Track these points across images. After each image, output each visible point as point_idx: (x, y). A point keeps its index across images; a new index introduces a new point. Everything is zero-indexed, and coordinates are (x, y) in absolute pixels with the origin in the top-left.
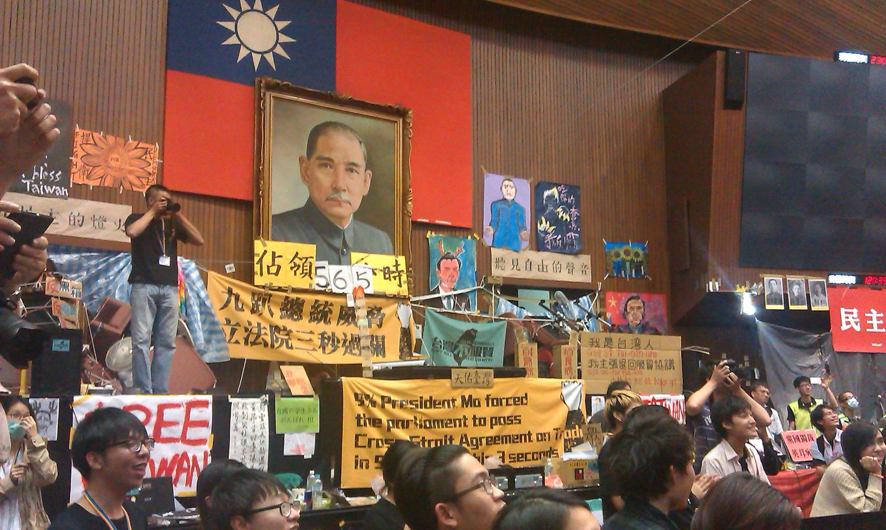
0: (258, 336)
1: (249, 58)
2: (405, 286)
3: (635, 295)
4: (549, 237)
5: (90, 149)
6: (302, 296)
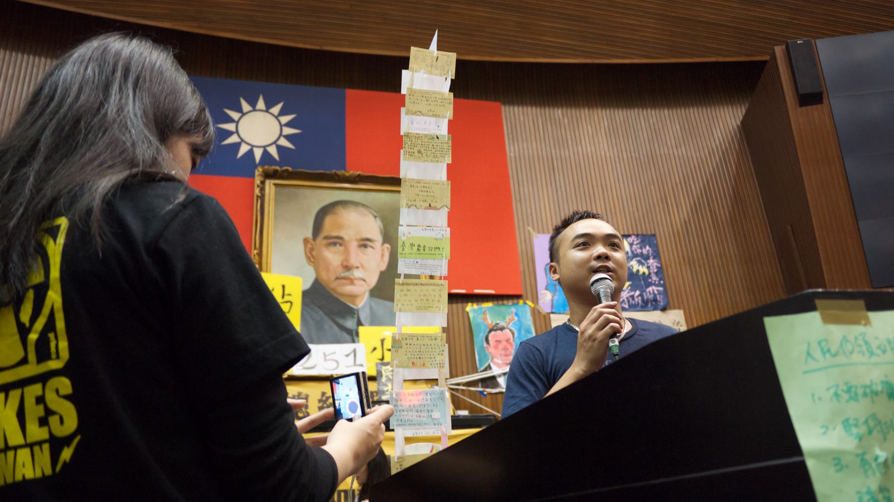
1: (250, 153)
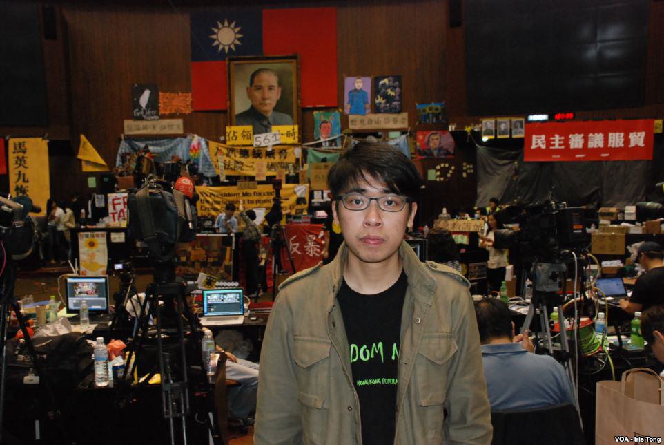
0: (229, 166)
1: (224, 49)
2: (297, 140)
3: (434, 132)
4: (382, 106)
5: (165, 100)
6: (247, 148)
